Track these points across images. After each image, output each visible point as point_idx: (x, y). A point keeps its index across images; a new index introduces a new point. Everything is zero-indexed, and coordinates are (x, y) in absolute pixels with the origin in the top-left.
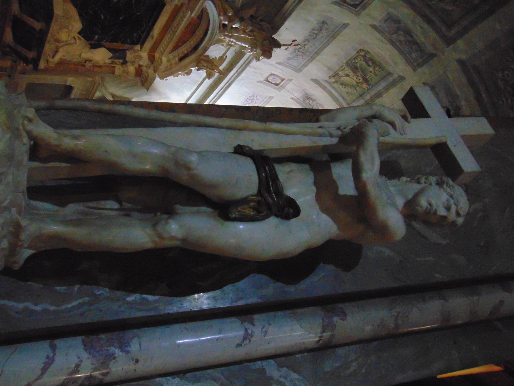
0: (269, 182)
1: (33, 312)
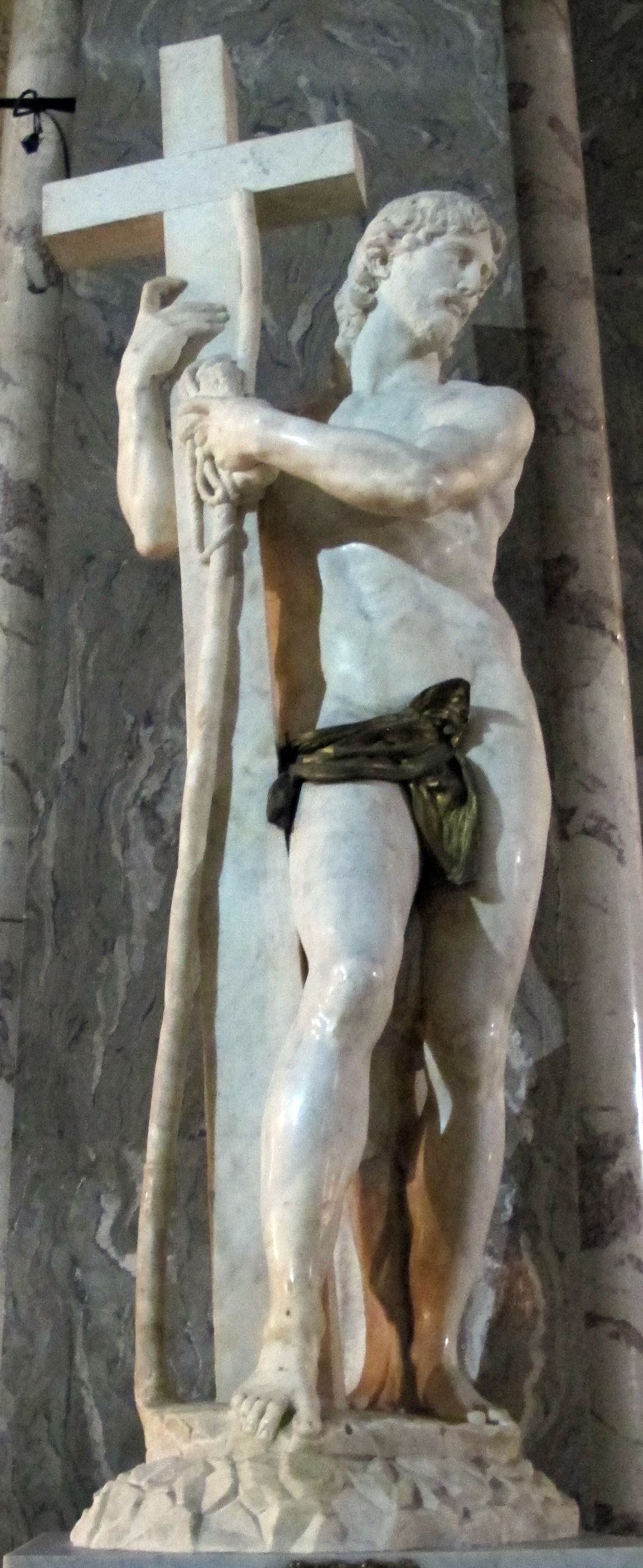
1: (548, 1374)
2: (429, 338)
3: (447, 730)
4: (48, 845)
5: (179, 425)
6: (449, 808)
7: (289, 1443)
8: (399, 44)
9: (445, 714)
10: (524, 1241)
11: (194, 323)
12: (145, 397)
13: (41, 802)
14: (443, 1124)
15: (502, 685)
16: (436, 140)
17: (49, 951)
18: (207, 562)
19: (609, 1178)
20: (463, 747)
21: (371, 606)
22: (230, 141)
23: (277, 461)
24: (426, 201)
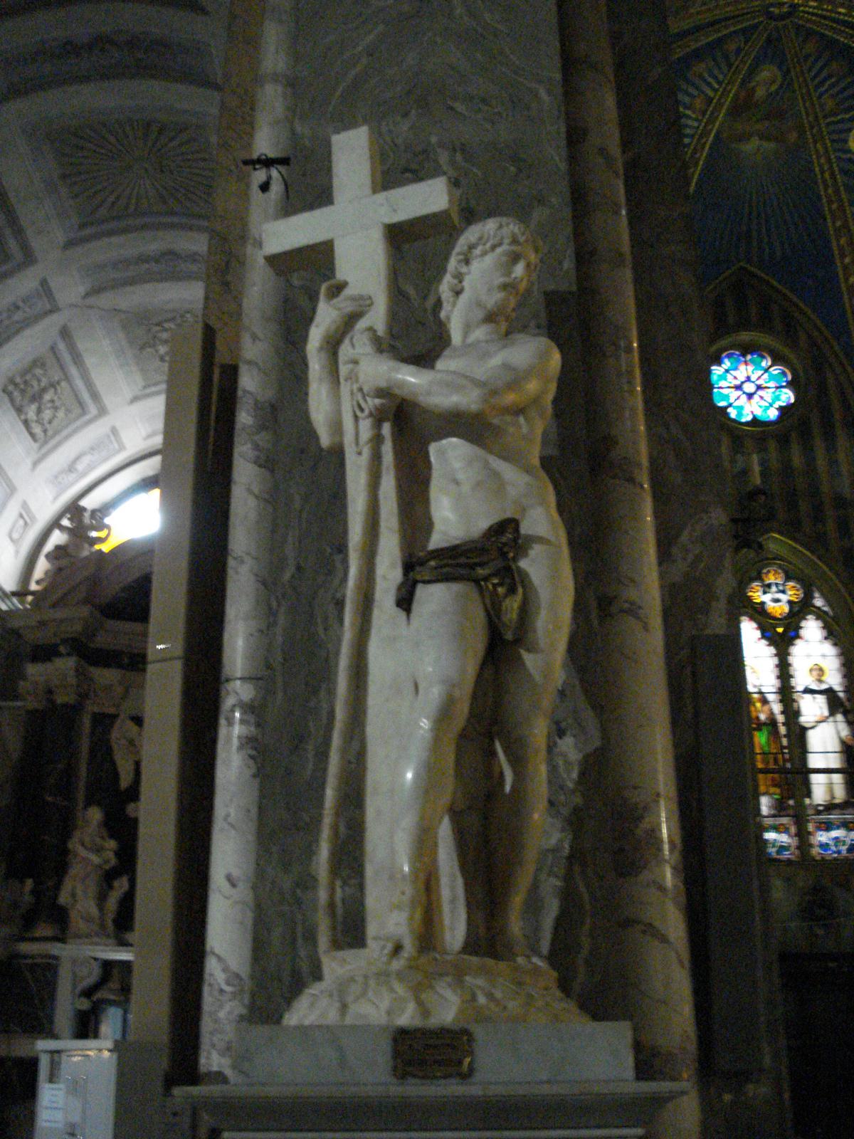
0: (457, 563)
2: (495, 309)
3: (505, 550)
4: (278, 631)
5: (344, 370)
6: (506, 596)
7: (397, 965)
8: (496, 110)
9: (504, 539)
10: (577, 869)
11: (349, 308)
12: (323, 355)
13: (274, 604)
14: (508, 788)
15: (541, 520)
16: (520, 170)
17: (280, 695)
18: (360, 453)
19: (639, 832)
20: (515, 559)
21: (461, 476)
22: (375, 191)
23: (397, 391)
24: (490, 225)
